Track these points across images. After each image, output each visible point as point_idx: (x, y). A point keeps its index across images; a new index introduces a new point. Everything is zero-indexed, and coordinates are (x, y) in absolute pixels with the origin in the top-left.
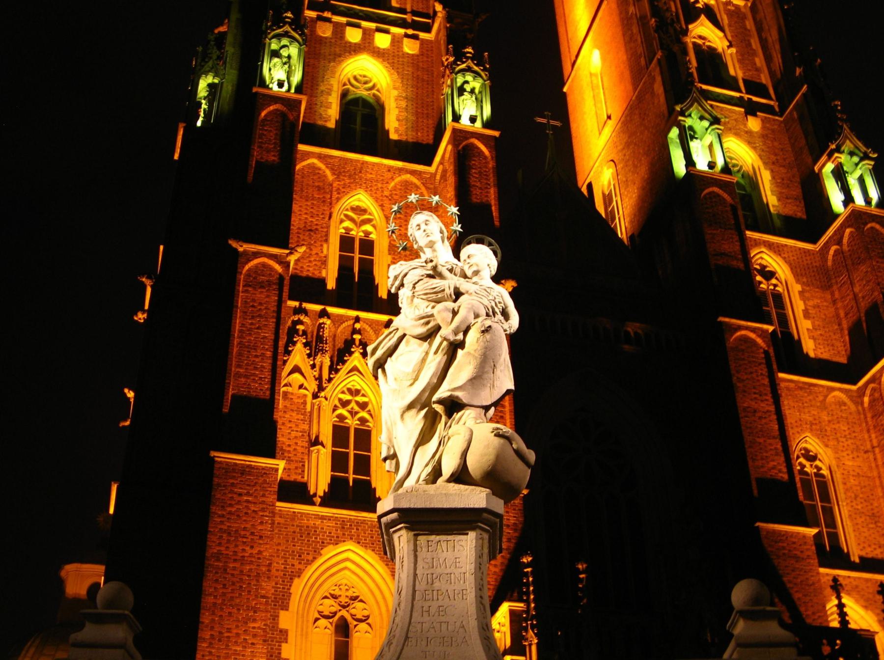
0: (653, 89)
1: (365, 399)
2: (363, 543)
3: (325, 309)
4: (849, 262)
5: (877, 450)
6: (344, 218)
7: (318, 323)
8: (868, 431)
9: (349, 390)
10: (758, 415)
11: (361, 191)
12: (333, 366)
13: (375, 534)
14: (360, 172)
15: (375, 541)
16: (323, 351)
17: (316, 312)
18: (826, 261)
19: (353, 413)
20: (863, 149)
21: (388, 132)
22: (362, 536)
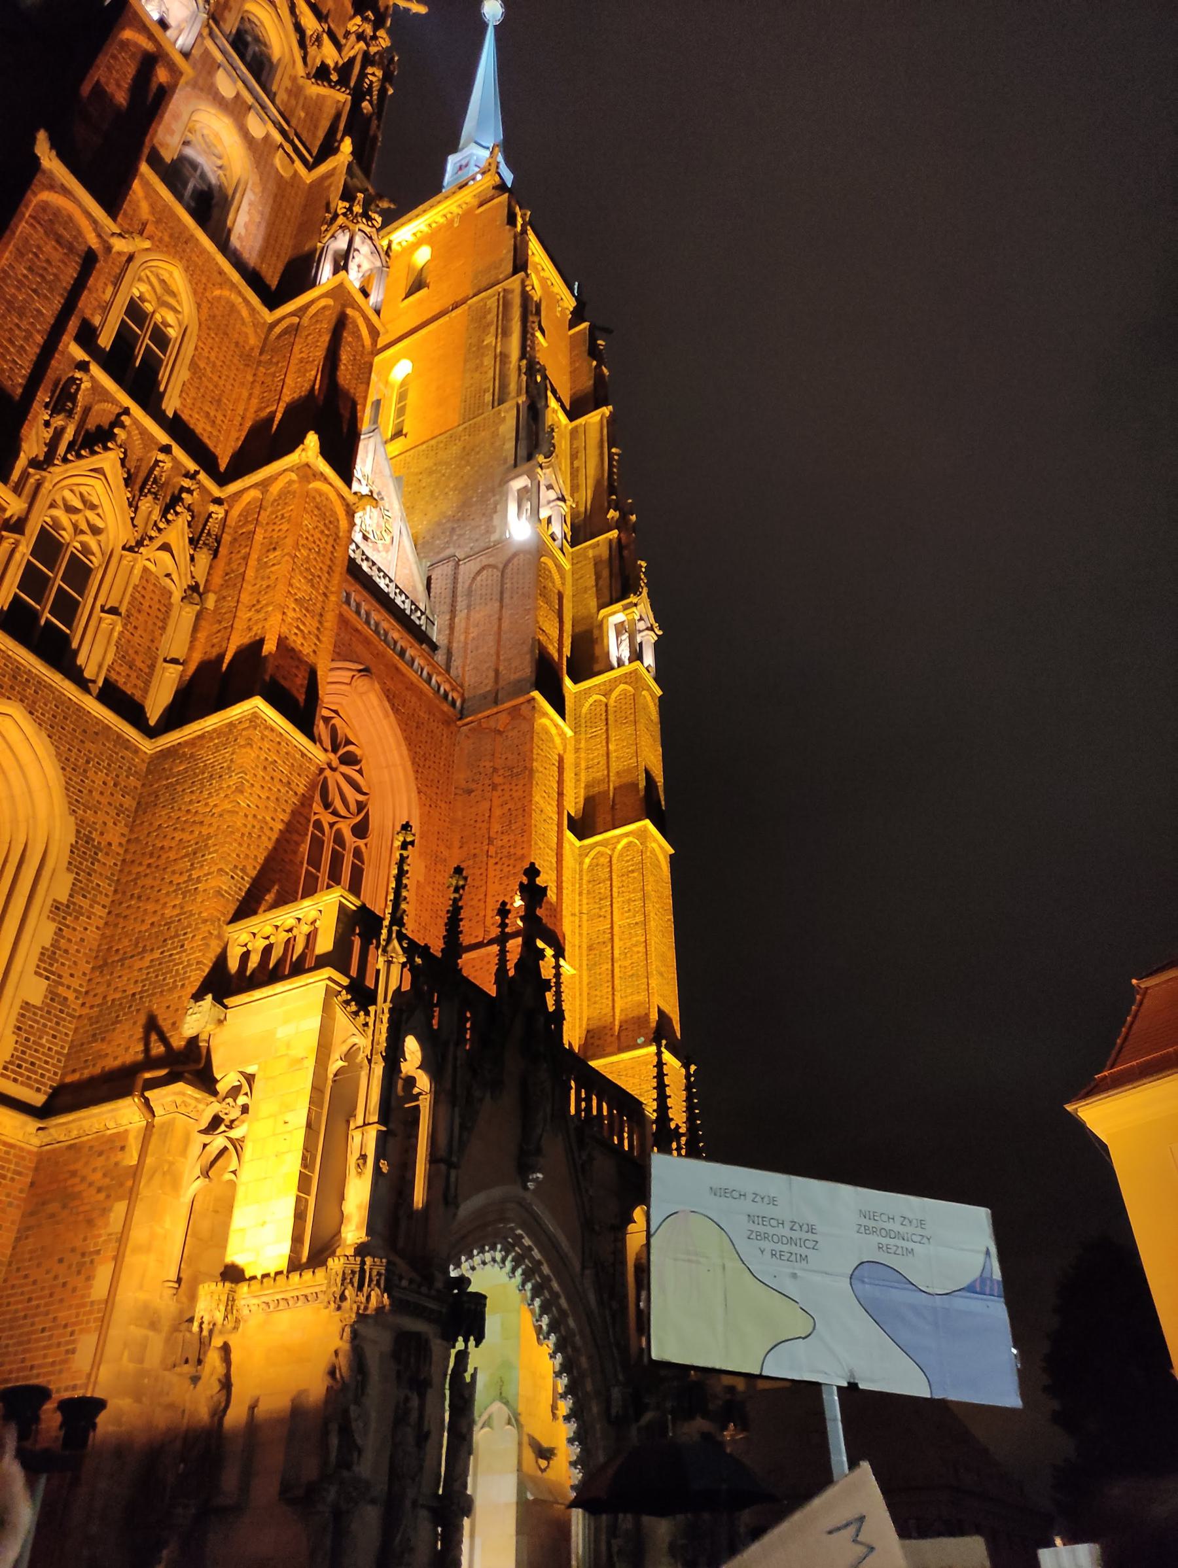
0: (498, 429)
1: (100, 524)
2: (37, 717)
3: (88, 363)
4: (611, 717)
5: (585, 917)
6: (145, 278)
7: (70, 375)
8: (580, 894)
9: (81, 494)
10: (544, 816)
11: (180, 266)
12: (75, 445)
13: (60, 714)
14: (186, 243)
15: (57, 724)
16: (70, 414)
17: (73, 358)
18: (581, 706)
19: (78, 531)
20: (653, 621)
21: (230, 231)
22: (40, 707)
